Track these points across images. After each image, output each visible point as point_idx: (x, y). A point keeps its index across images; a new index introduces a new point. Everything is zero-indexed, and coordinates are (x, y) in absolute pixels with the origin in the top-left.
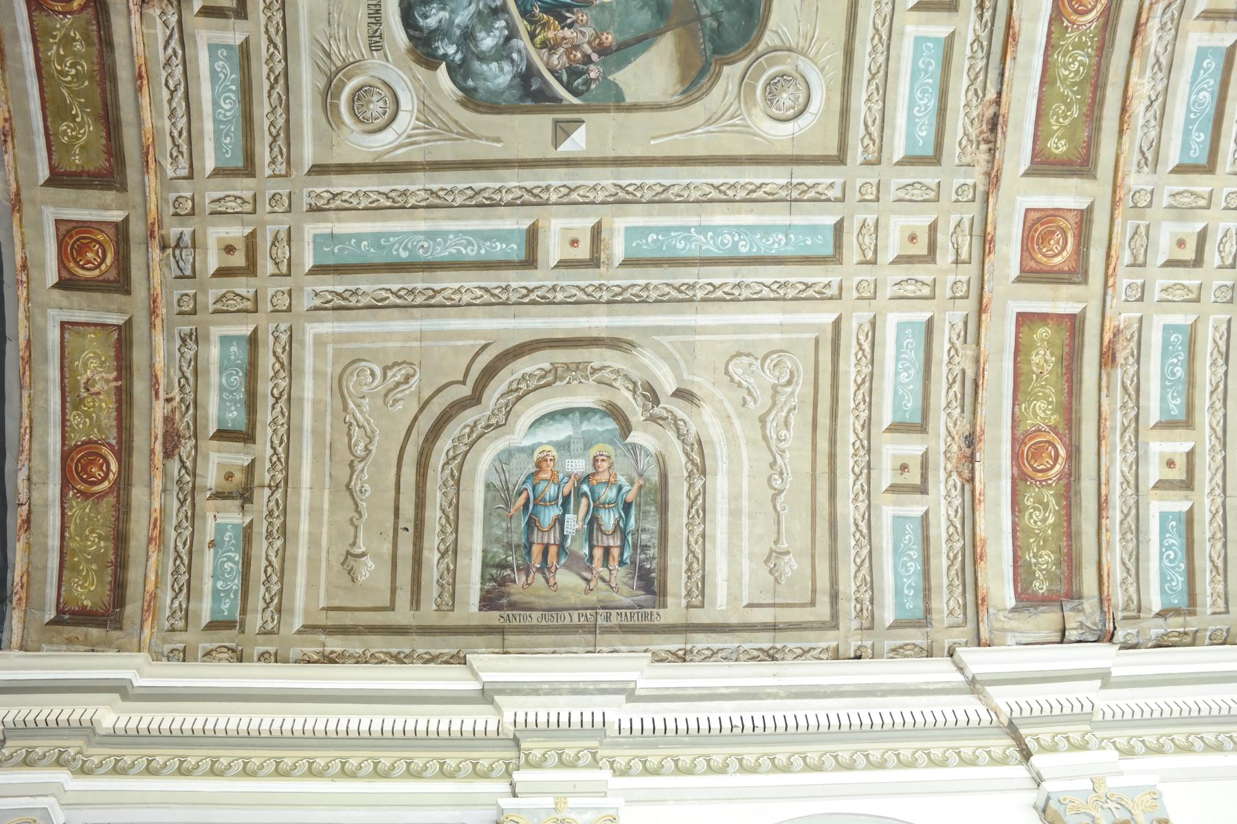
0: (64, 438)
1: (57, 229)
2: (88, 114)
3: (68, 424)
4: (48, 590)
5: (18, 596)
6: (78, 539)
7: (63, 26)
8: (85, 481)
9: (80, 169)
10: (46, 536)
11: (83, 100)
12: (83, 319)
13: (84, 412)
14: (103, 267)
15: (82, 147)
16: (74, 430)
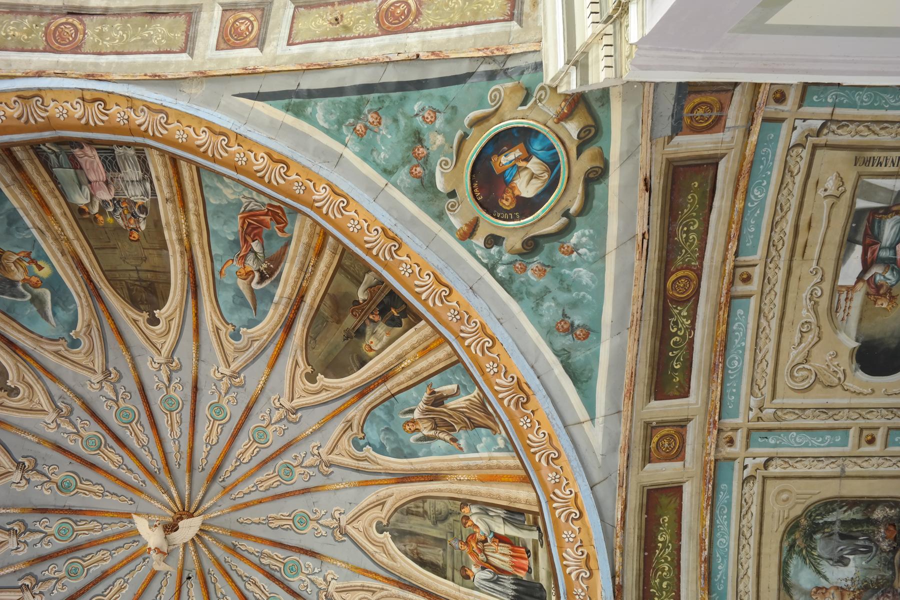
0: (374, 36)
1: (222, 49)
2: (149, 27)
3: (361, 34)
4: (493, 31)
5: (495, 51)
6: (452, 15)
7: (92, 35)
8: (407, 17)
9: (184, 33)
10: (449, 40)
11: (140, 28)
12: (288, 31)
13: (353, 25)
14: (252, 19)
15: (171, 31)
16: (368, 29)
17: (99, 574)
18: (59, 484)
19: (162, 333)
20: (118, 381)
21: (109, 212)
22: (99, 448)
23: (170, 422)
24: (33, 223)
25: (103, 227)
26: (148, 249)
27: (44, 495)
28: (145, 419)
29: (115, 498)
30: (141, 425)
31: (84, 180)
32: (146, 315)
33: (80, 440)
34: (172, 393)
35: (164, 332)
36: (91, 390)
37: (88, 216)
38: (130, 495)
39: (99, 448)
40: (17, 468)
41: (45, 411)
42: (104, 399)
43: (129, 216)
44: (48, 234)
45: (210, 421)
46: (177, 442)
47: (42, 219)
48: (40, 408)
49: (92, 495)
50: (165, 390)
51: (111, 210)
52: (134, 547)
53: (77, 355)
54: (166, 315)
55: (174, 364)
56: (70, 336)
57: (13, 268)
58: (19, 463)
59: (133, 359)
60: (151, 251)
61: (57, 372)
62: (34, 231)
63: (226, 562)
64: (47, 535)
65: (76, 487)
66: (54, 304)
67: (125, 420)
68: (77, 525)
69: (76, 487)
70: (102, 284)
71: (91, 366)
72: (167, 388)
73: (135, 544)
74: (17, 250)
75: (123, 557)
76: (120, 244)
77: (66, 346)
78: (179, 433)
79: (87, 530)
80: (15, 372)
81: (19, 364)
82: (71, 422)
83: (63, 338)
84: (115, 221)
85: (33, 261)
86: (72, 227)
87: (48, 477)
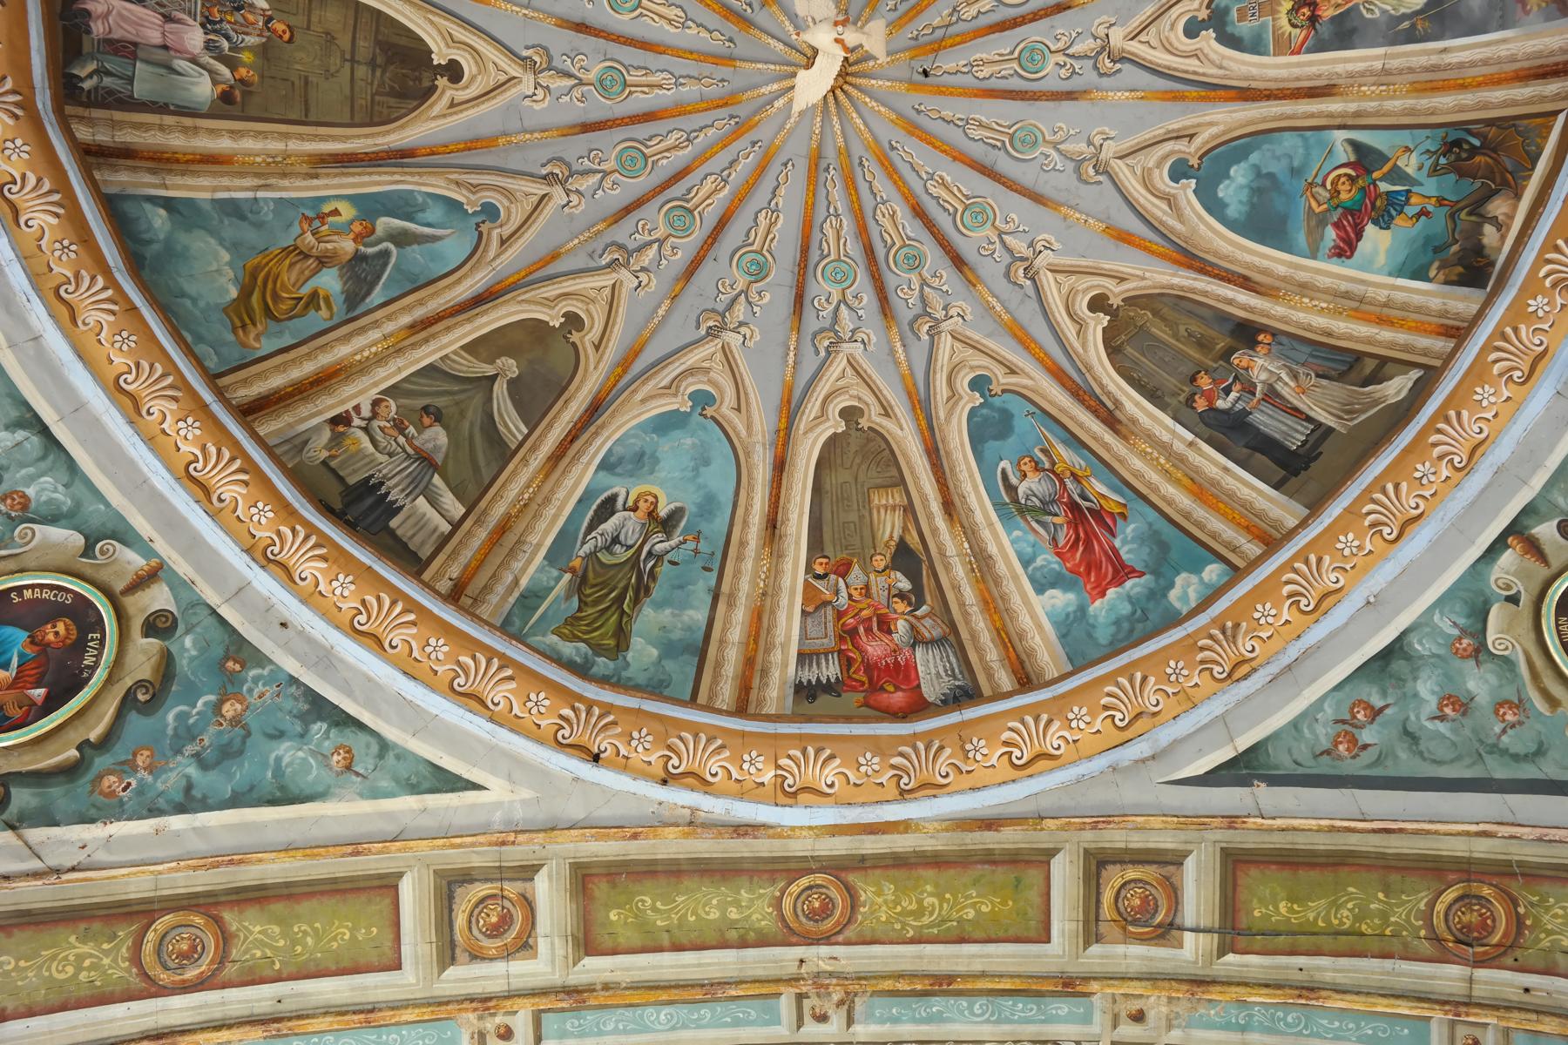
17: (918, 223)
18: (752, 279)
19: (476, 62)
20: (568, 165)
21: (230, 49)
22: (691, 212)
23: (646, 89)
24: (247, 189)
25: (262, 77)
26: (309, 21)
27: (771, 302)
28: (641, 131)
29: (782, 191)
30: (650, 140)
31: (161, 55)
32: (442, 82)
33: (672, 239)
34: (592, 76)
35: (474, 58)
36: (581, 208)
37: (237, 93)
38: (775, 167)
39: (691, 212)
40: (717, 337)
41: (614, 285)
42: (600, 192)
43: (238, 17)
44: (272, 181)
45: (641, 15)
46: (681, 80)
47: (242, 175)
48: (607, 291)
49: (774, 230)
50: (586, 88)
51: (225, 44)
52: (871, 165)
53: (513, 216)
54: (442, 45)
55: (537, 58)
56: (475, 213)
57: (329, 246)
58: (708, 334)
59: (525, 131)
60: (314, 19)
61: (543, 250)
62: (260, 194)
63: (896, 9)
64: (843, 301)
65: (760, 252)
66: (409, 218)
67: (641, 163)
68: (829, 255)
69: (760, 252)
70: (380, 140)
71: (535, 199)
72: (581, 83)
73: (866, 164)
74: (296, 230)
75: (889, 184)
76: (298, 67)
77: (492, 225)
78: (666, 75)
79: (839, 237)
80: (533, 307)
81: (520, 299)
82: (639, 249)
83: (478, 225)
84: (249, 48)
85: (322, 217)
86: (260, 133)
87: (739, 295)
